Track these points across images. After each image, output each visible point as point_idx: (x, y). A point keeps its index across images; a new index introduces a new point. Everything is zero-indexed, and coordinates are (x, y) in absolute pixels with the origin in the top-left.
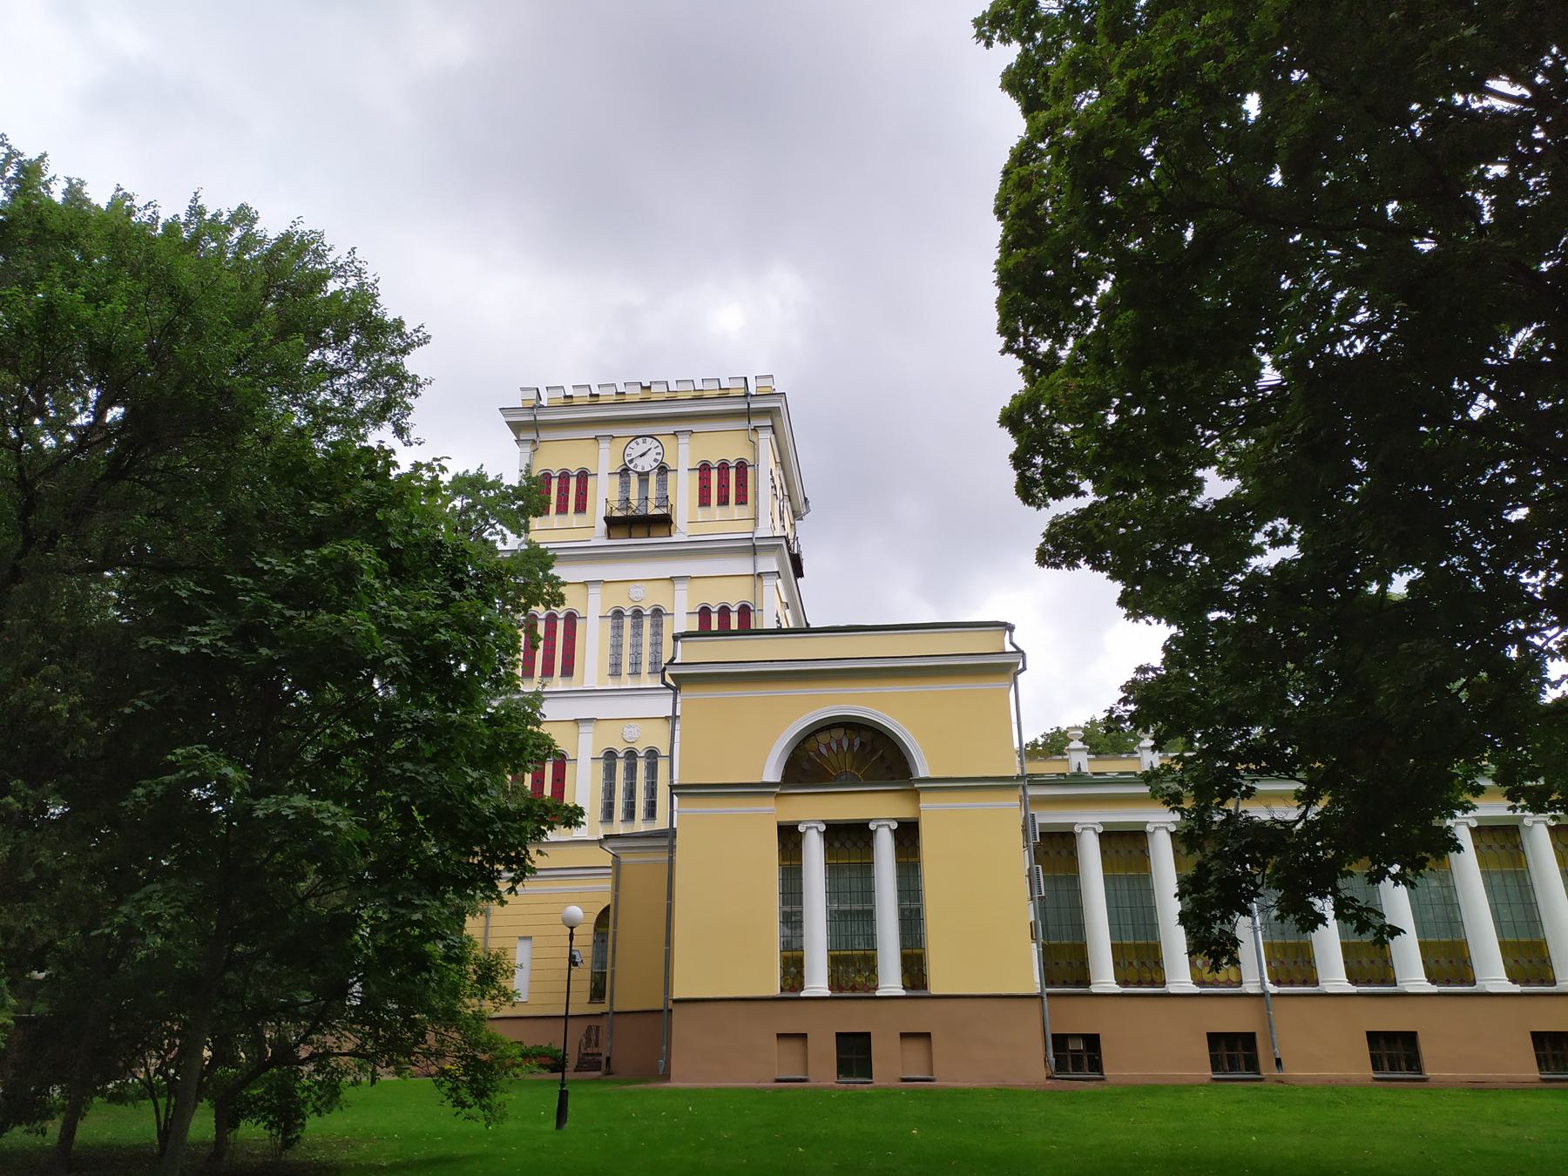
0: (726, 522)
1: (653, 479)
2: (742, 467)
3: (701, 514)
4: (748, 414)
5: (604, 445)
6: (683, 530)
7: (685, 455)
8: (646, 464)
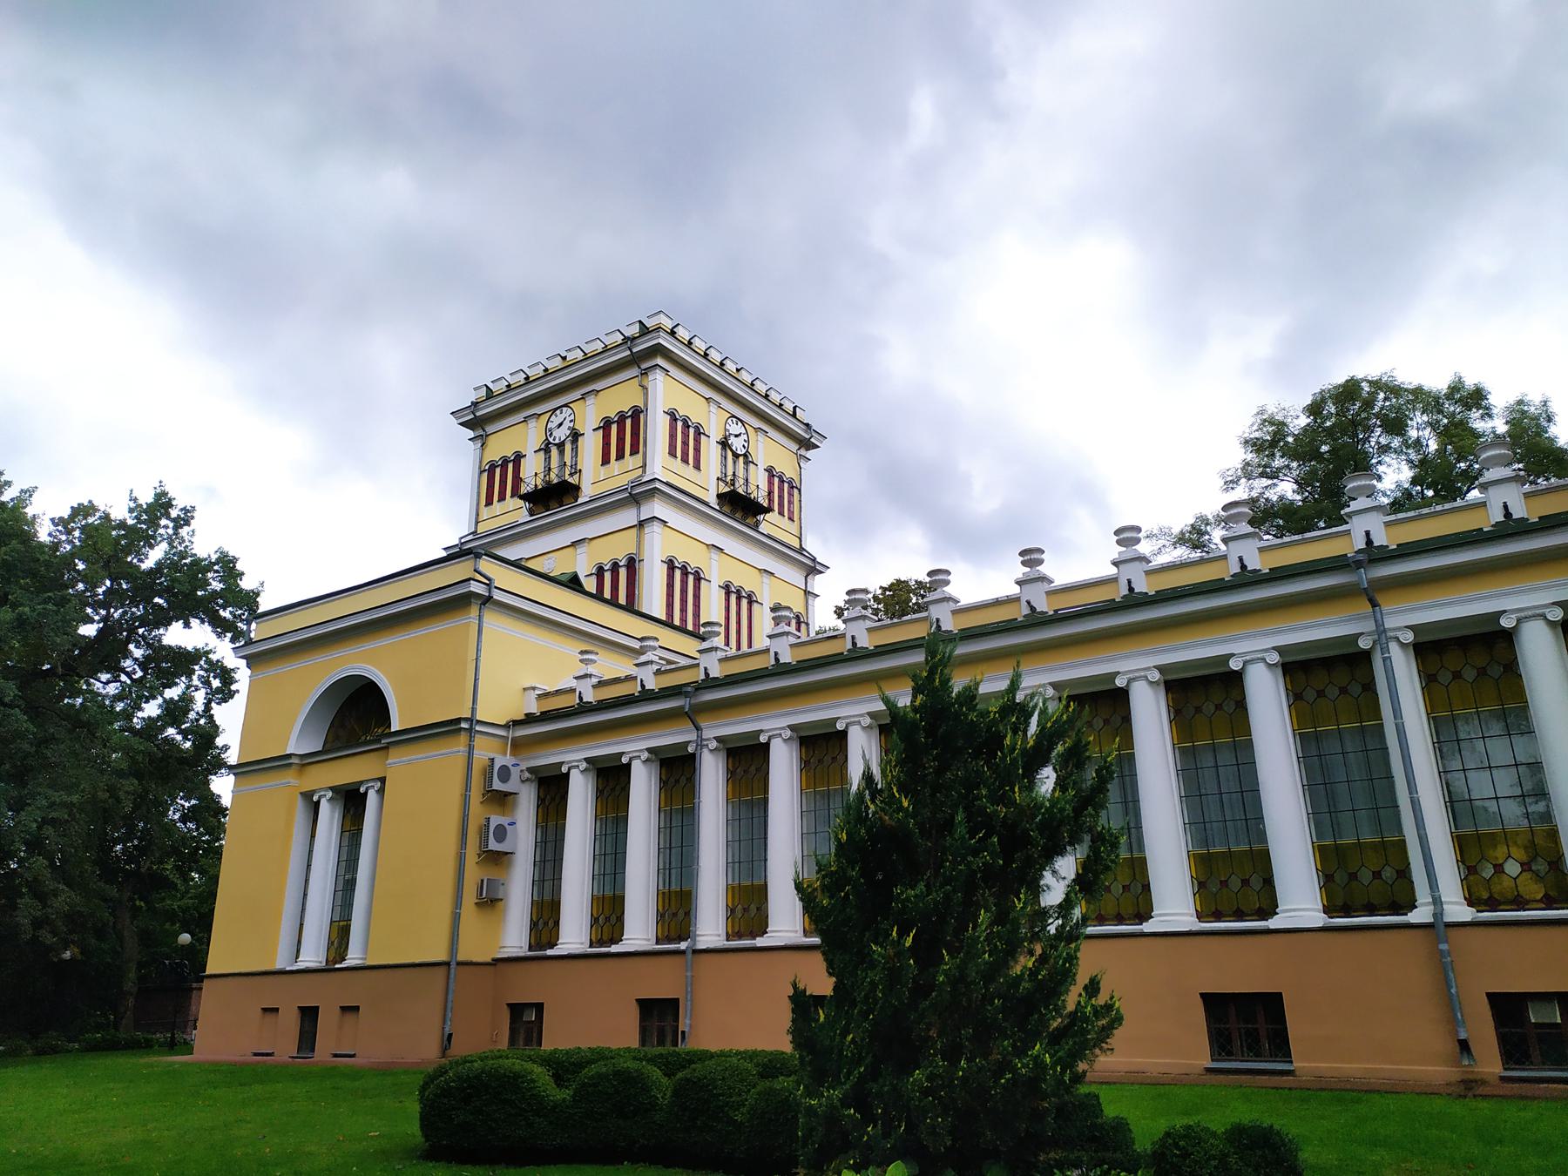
0: (621, 473)
1: (568, 447)
2: (636, 413)
3: (603, 472)
4: (634, 360)
5: (532, 423)
6: (588, 491)
7: (590, 414)
8: (561, 434)
